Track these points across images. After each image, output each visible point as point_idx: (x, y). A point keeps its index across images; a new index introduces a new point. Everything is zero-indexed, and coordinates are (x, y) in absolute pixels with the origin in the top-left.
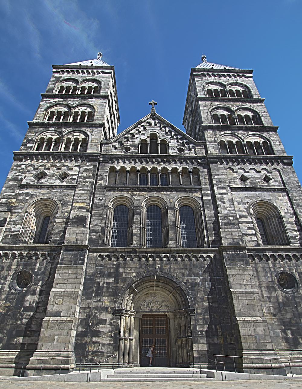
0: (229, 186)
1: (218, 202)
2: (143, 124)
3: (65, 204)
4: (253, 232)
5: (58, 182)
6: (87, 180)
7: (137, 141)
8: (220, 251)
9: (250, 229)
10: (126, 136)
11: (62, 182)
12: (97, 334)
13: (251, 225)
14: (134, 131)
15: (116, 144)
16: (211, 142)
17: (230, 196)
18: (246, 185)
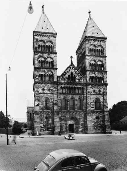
0: (90, 94)
1: (87, 99)
2: (69, 68)
3: (51, 99)
4: (93, 107)
5: (48, 92)
6: (56, 91)
7: (67, 76)
8: (86, 111)
9: (93, 106)
10: (64, 74)
11: (49, 92)
12: (63, 128)
13: (93, 105)
14: (66, 72)
15: (61, 77)
16: (88, 77)
17: (90, 97)
18: (94, 93)
